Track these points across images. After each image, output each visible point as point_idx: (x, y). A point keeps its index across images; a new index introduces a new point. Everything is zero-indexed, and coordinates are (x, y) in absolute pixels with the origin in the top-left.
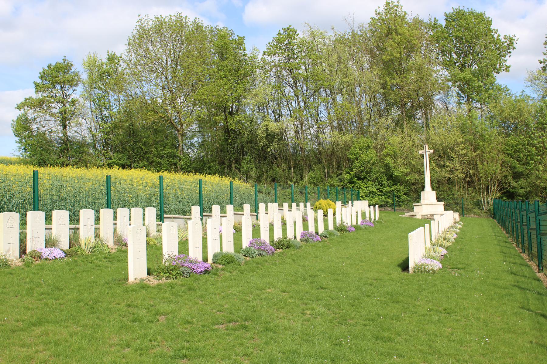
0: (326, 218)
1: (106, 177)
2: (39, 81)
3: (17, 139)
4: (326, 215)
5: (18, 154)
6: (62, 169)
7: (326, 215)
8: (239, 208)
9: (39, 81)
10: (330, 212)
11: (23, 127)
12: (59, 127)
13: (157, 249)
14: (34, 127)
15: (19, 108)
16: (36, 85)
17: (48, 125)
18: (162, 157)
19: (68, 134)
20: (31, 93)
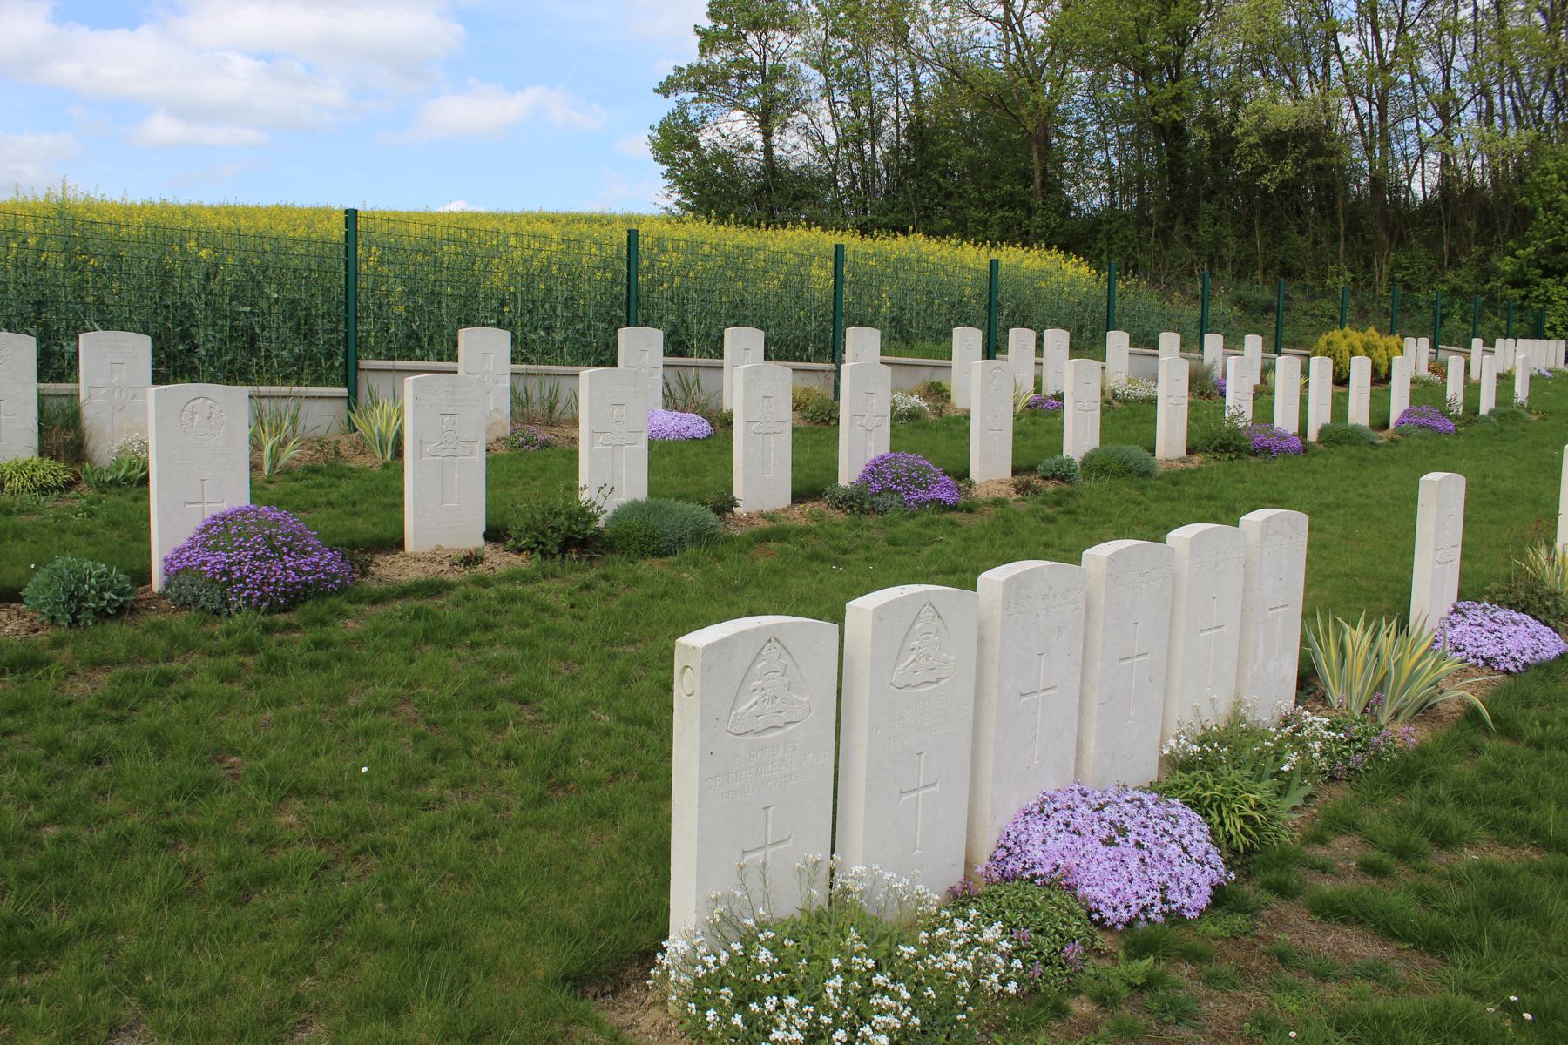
0: (1342, 389)
1: (625, 236)
2: (707, 24)
3: (665, 169)
4: (1341, 380)
5: (670, 203)
6: (721, 228)
7: (1341, 380)
8: (1145, 341)
9: (707, 24)
10: (1360, 369)
11: (674, 140)
12: (776, 142)
13: (259, 497)
14: (704, 139)
15: (666, 89)
16: (704, 34)
17: (730, 128)
18: (989, 206)
19: (777, 152)
20: (689, 55)
